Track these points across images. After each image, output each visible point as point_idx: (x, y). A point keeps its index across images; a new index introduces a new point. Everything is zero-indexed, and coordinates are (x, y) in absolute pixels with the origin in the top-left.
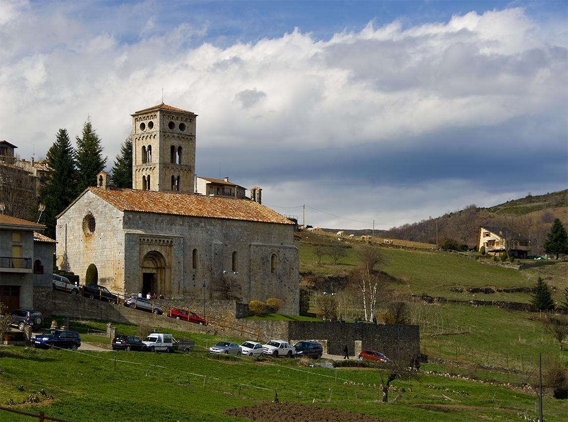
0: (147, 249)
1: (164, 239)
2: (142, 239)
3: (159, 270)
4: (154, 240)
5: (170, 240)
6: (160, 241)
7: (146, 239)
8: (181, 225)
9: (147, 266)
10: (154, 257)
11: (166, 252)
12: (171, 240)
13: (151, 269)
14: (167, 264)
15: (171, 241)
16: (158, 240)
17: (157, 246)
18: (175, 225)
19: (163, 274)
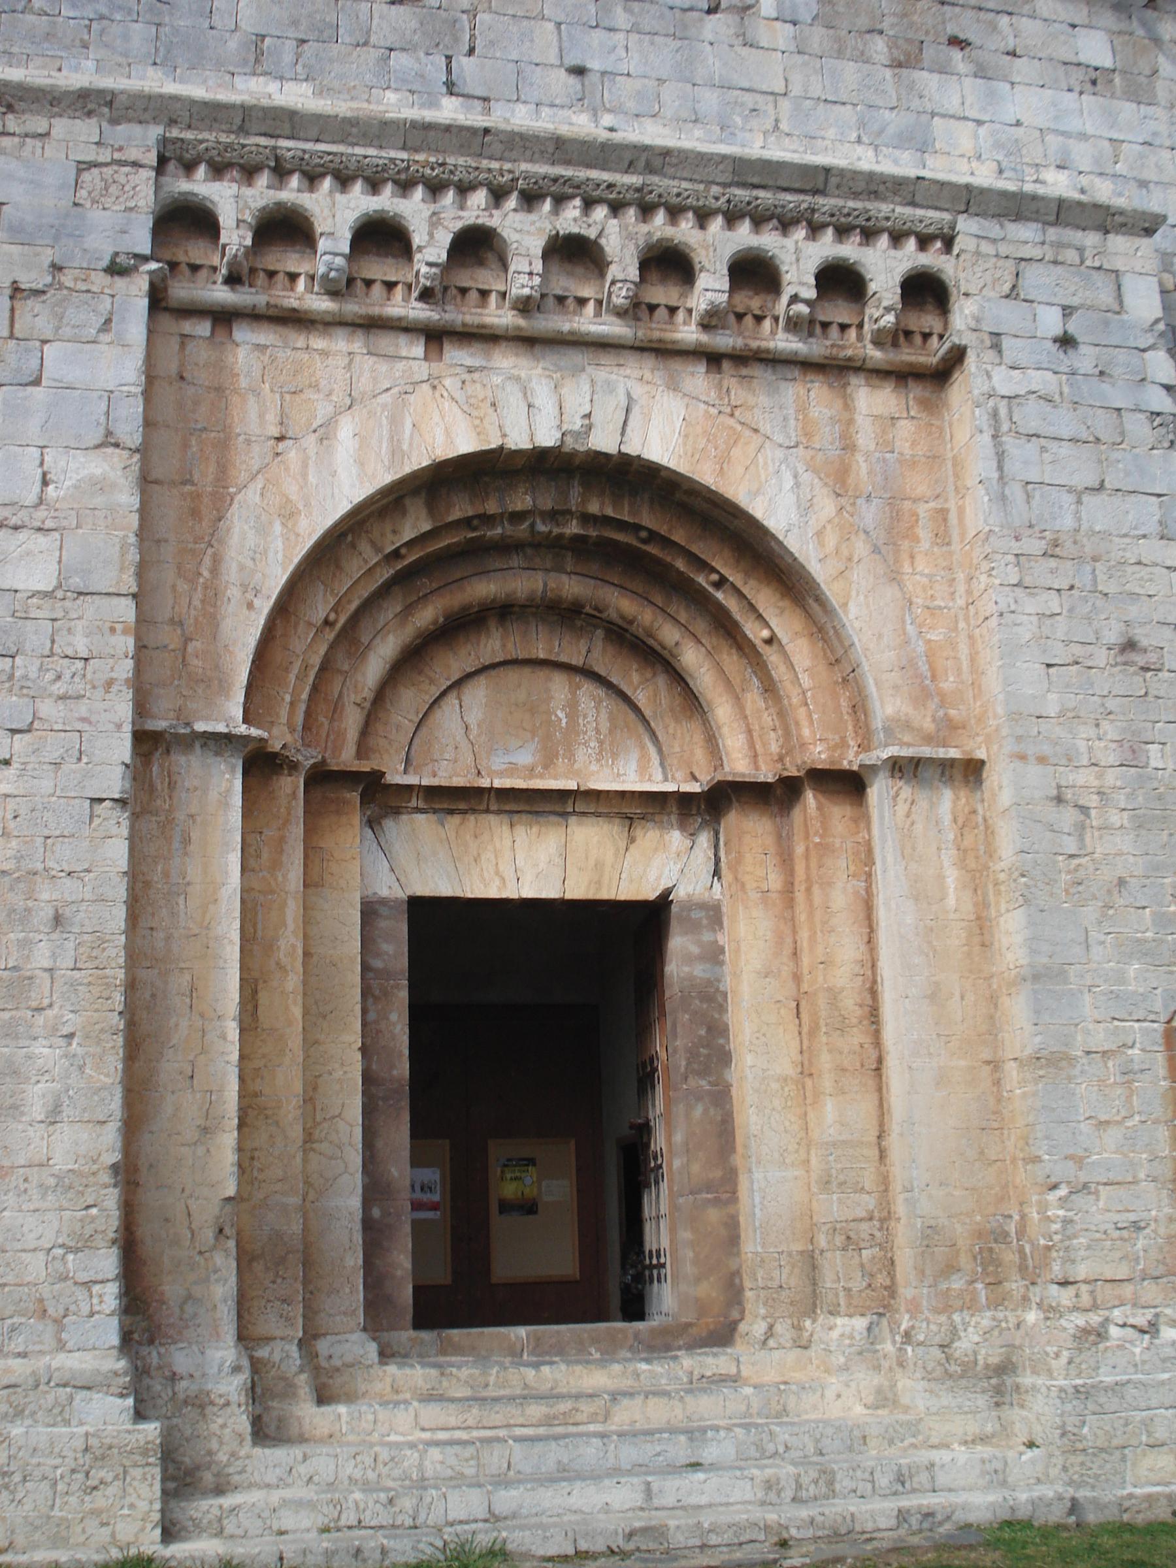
0: (348, 428)
1: (744, 236)
2: (234, 204)
3: (749, 829)
4: (525, 233)
5: (885, 268)
6: (669, 263)
7: (336, 213)
8: (1095, 80)
9: (513, 766)
10: (622, 604)
11: (839, 478)
12: (909, 257)
13: (591, 837)
14: (886, 706)
15: (925, 290)
16: (623, 265)
17: (630, 378)
18: (982, 72)
19: (841, 897)
